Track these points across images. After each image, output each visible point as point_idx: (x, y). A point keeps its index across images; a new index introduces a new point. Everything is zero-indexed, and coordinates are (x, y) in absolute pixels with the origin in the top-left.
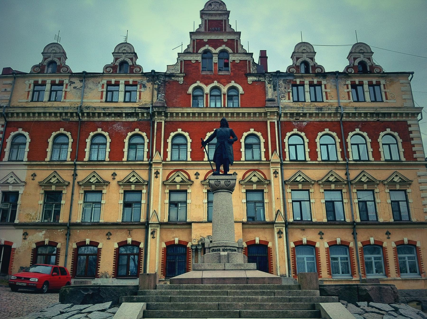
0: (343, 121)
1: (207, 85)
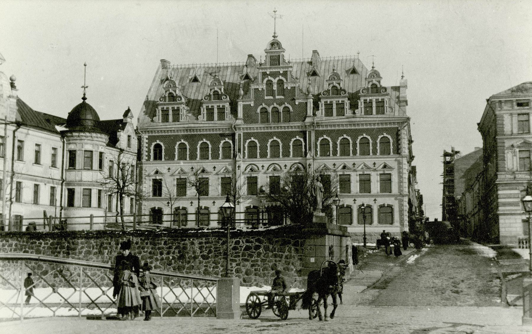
1: (269, 106)
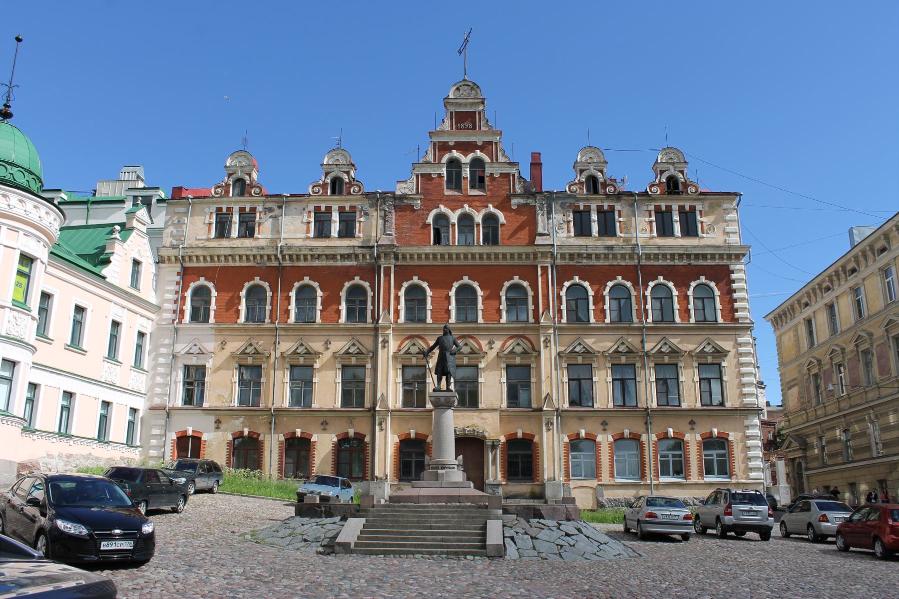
0: (642, 266)
1: (453, 210)
